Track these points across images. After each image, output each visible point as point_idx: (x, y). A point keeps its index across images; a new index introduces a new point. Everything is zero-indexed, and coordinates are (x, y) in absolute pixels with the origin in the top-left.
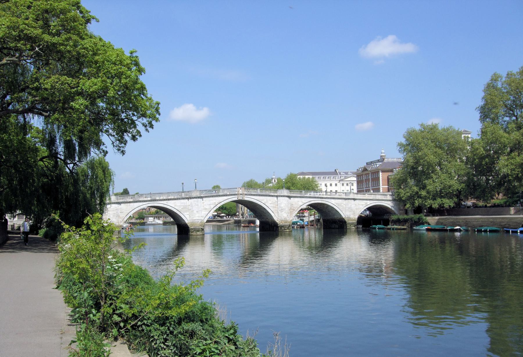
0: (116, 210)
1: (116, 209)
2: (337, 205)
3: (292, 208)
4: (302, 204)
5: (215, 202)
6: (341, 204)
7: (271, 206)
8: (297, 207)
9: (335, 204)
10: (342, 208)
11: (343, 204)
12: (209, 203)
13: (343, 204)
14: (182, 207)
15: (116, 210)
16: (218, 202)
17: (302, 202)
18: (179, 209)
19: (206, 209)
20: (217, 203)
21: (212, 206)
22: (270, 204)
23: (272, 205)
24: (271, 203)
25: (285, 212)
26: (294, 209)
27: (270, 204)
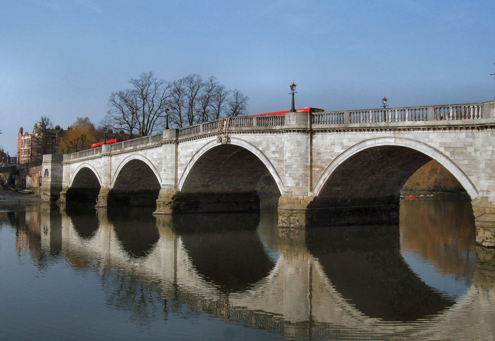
0: (105, 166)
1: (104, 164)
2: (448, 154)
3: (319, 163)
4: (342, 151)
5: (192, 150)
6: (465, 147)
7: (275, 159)
8: (328, 160)
9: (442, 150)
10: (466, 162)
11: (470, 149)
12: (185, 154)
13: (470, 149)
14: (158, 162)
15: (105, 166)
16: (196, 150)
17: (342, 144)
18: (156, 164)
19: (182, 165)
20: (194, 153)
21: (189, 159)
22: (274, 152)
23: (277, 155)
24: (273, 149)
25: (290, 175)
26: (323, 165)
27: (274, 152)
